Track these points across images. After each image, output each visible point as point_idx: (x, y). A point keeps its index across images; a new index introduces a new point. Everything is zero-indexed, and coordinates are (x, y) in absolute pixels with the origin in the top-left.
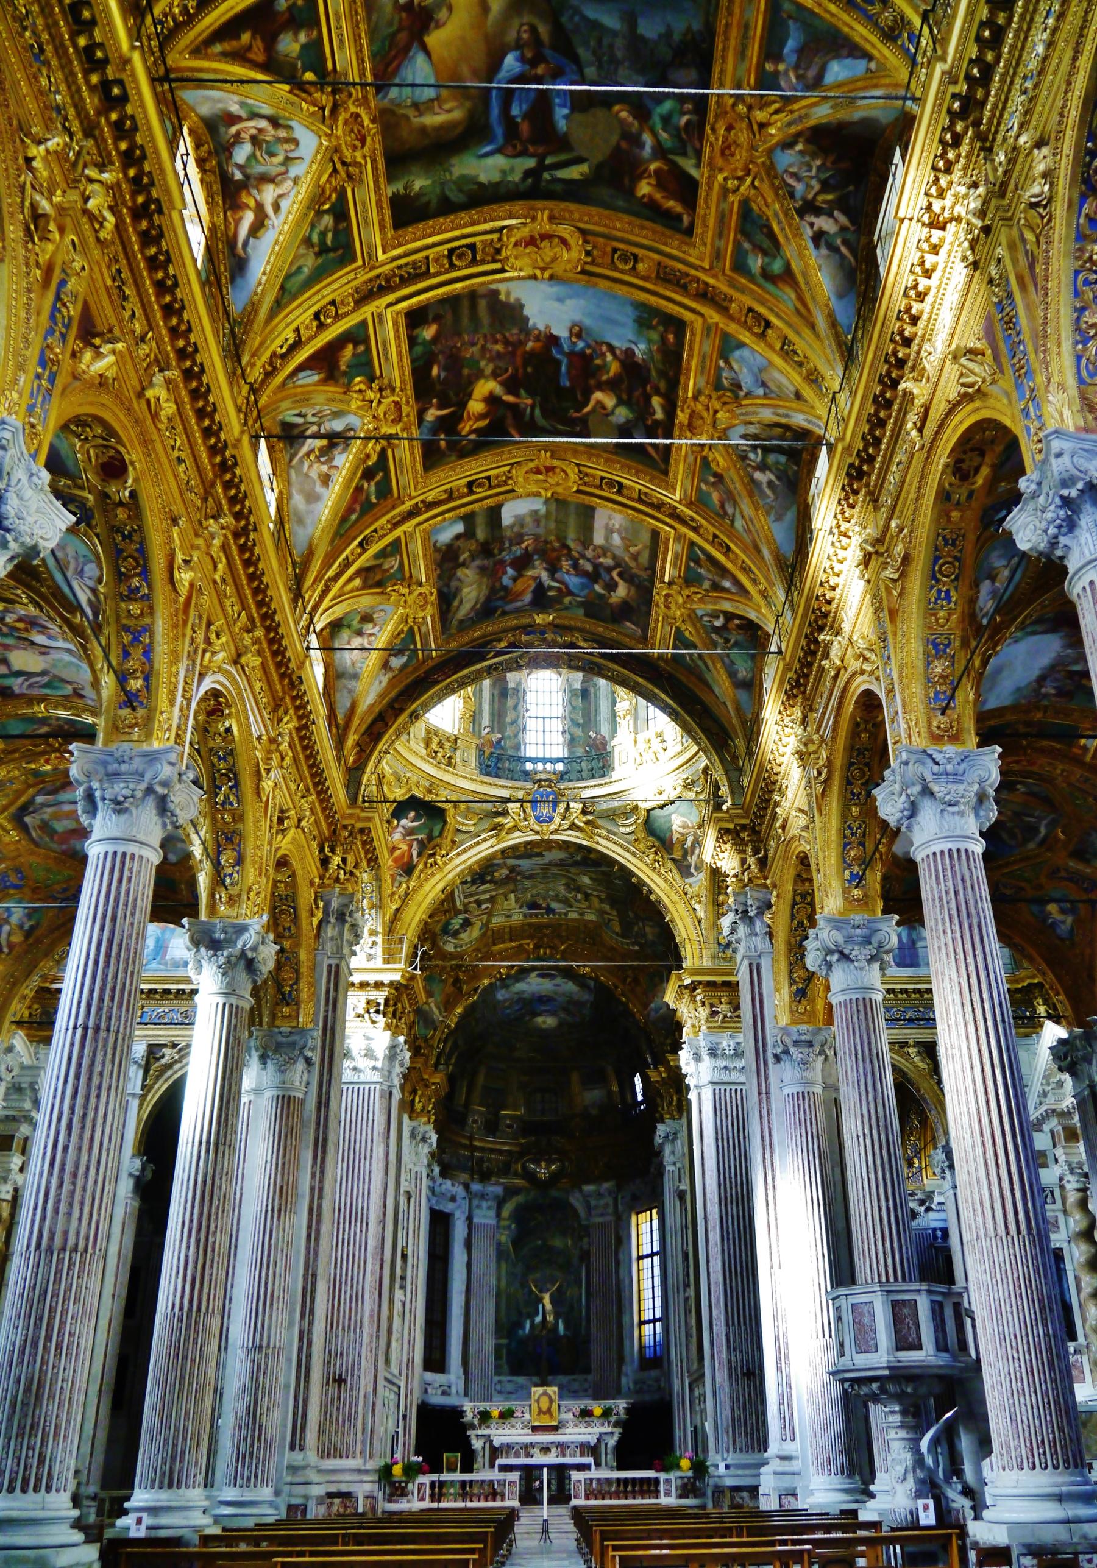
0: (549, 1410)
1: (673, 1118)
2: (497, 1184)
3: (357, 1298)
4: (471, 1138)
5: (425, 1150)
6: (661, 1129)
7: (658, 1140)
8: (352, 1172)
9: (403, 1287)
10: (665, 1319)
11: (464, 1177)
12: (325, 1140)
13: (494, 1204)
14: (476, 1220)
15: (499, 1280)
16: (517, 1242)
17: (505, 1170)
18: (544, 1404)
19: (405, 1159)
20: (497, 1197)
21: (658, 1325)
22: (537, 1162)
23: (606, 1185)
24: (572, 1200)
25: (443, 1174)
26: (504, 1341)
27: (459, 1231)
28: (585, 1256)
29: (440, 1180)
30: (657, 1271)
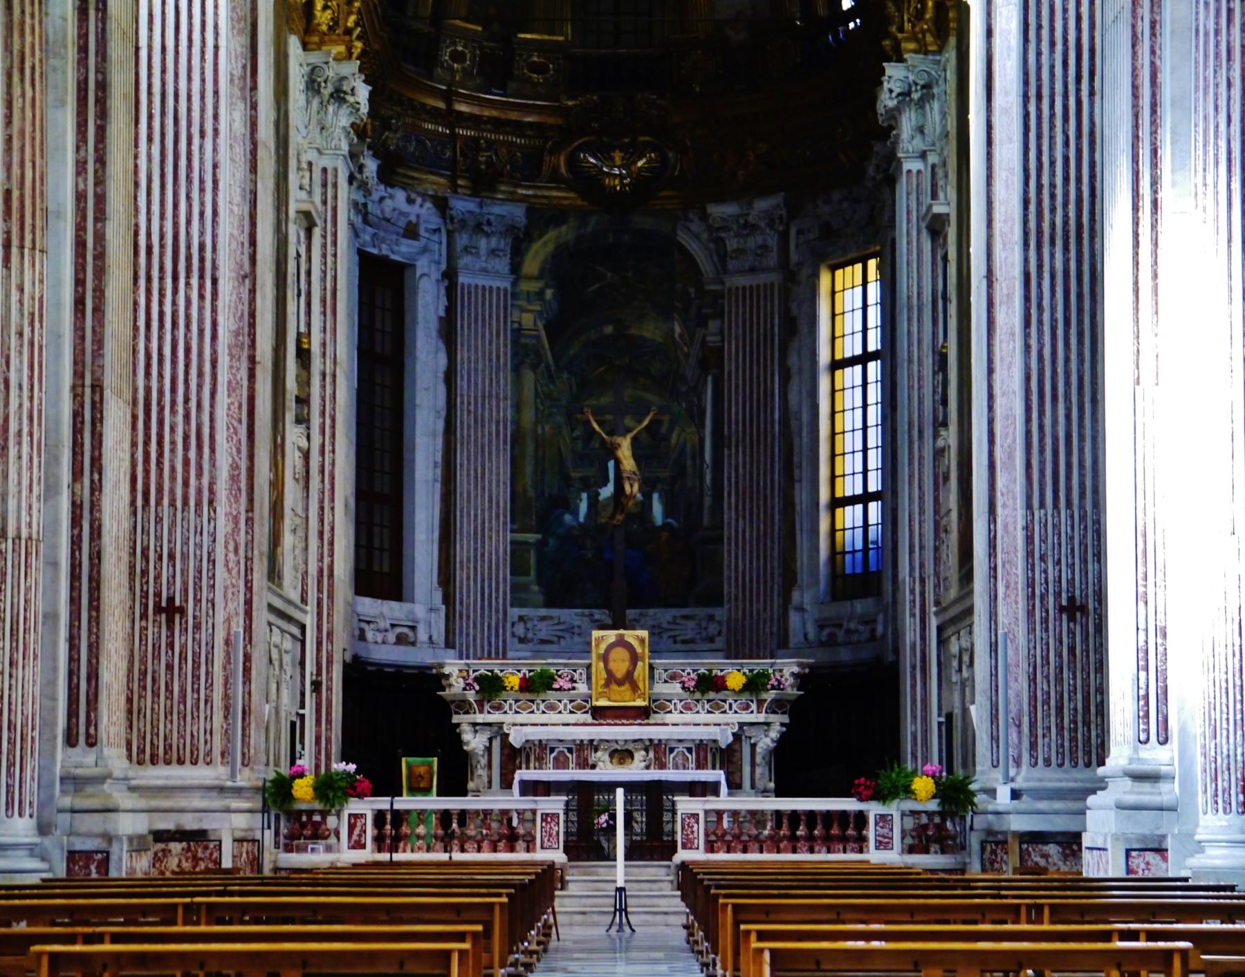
0: (629, 678)
1: (923, 50)
2: (513, 199)
3: (202, 441)
4: (448, 96)
5: (343, 119)
6: (895, 75)
7: (887, 101)
8: (178, 168)
9: (302, 420)
10: (888, 496)
11: (435, 182)
12: (102, 86)
13: (505, 244)
14: (461, 279)
15: (518, 407)
16: (556, 328)
17: (530, 168)
18: (620, 664)
19: (296, 139)
20: (511, 229)
21: (874, 507)
22: (604, 153)
23: (762, 205)
24: (684, 238)
25: (386, 176)
26: (531, 537)
27: (427, 302)
28: (712, 360)
29: (380, 190)
30: (874, 393)
